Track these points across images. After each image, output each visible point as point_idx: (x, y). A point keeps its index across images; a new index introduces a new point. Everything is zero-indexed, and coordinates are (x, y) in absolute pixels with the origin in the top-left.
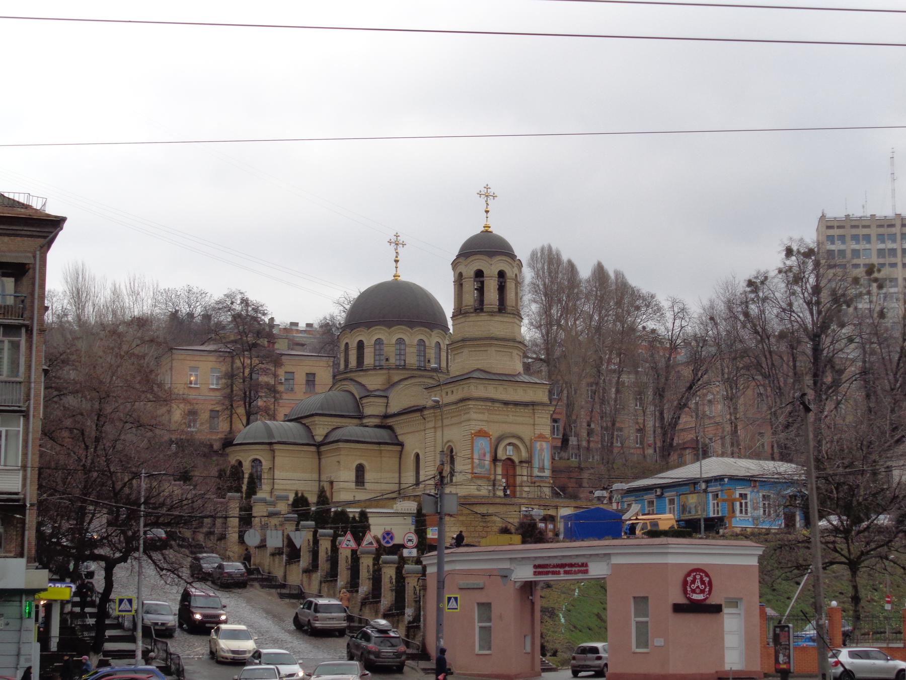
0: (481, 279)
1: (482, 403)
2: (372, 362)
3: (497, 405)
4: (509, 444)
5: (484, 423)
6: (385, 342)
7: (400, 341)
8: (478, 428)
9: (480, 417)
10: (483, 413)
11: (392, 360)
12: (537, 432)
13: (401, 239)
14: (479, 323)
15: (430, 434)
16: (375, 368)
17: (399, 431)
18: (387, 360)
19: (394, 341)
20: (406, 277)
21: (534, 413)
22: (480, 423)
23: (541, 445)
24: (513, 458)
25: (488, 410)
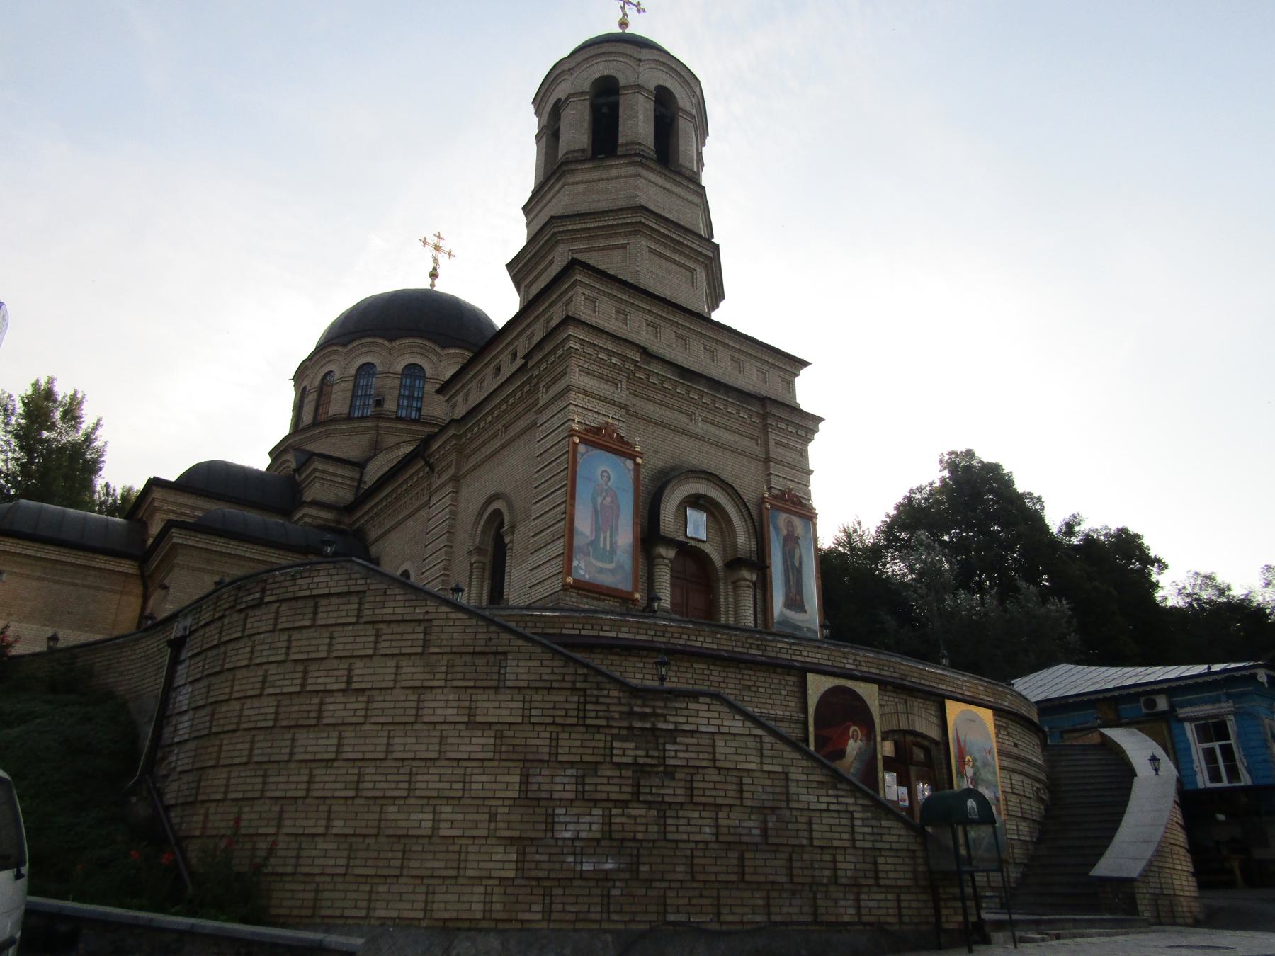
0: (612, 99)
1: (610, 346)
2: (346, 410)
3: (656, 368)
4: (696, 501)
5: (615, 412)
6: (379, 369)
7: (413, 371)
8: (594, 421)
9: (605, 389)
10: (616, 385)
11: (390, 405)
12: (777, 484)
13: (446, 246)
14: (602, 185)
15: (441, 502)
16: (349, 418)
17: (373, 534)
18: (379, 403)
19: (399, 368)
20: (442, 287)
21: (765, 427)
22: (601, 407)
23: (790, 524)
24: (707, 548)
25: (631, 377)
